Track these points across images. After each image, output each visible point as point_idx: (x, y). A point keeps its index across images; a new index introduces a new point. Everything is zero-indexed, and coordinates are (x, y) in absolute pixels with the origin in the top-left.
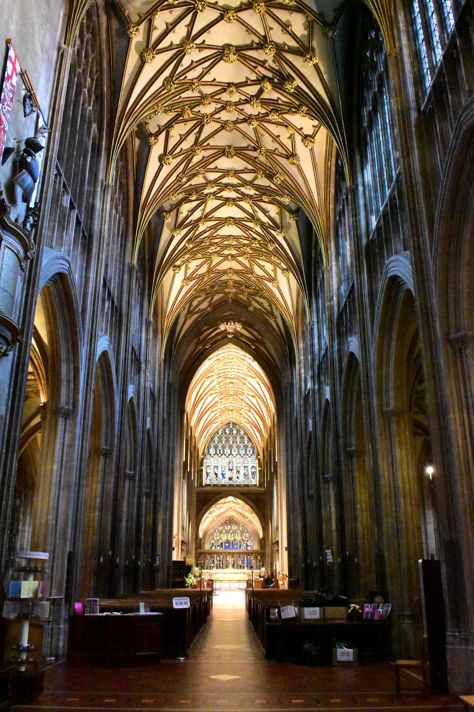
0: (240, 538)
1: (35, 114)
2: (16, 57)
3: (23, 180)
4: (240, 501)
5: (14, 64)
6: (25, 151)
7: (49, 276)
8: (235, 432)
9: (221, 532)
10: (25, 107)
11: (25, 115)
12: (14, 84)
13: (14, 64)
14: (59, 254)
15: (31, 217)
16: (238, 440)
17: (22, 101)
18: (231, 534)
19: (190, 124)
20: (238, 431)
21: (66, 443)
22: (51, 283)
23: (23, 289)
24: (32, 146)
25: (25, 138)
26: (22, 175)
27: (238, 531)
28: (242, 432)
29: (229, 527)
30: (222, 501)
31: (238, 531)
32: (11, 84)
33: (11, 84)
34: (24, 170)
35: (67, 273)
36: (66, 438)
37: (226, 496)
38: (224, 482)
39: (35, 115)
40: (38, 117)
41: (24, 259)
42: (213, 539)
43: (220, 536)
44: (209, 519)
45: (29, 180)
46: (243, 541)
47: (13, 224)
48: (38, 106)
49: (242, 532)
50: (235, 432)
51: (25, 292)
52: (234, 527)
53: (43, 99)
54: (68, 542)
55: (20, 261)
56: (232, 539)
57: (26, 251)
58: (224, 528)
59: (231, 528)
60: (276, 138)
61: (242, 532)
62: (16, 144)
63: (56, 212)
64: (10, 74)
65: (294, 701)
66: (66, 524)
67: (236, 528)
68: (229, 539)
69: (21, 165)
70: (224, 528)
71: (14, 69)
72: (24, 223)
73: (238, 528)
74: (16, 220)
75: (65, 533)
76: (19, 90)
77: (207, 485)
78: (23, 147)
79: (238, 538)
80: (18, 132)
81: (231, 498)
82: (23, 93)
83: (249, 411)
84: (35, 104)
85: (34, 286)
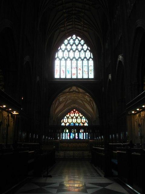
0: (80, 122)
9: (68, 118)
27: (79, 117)
29: (73, 115)
31: (79, 117)
42: (63, 122)
43: (68, 120)
46: (82, 123)
49: (81, 118)
52: (77, 115)
56: (75, 122)
58: (70, 115)
59: (75, 116)
61: (81, 118)
67: (77, 116)
68: (73, 122)
70: (70, 115)
73: (79, 115)
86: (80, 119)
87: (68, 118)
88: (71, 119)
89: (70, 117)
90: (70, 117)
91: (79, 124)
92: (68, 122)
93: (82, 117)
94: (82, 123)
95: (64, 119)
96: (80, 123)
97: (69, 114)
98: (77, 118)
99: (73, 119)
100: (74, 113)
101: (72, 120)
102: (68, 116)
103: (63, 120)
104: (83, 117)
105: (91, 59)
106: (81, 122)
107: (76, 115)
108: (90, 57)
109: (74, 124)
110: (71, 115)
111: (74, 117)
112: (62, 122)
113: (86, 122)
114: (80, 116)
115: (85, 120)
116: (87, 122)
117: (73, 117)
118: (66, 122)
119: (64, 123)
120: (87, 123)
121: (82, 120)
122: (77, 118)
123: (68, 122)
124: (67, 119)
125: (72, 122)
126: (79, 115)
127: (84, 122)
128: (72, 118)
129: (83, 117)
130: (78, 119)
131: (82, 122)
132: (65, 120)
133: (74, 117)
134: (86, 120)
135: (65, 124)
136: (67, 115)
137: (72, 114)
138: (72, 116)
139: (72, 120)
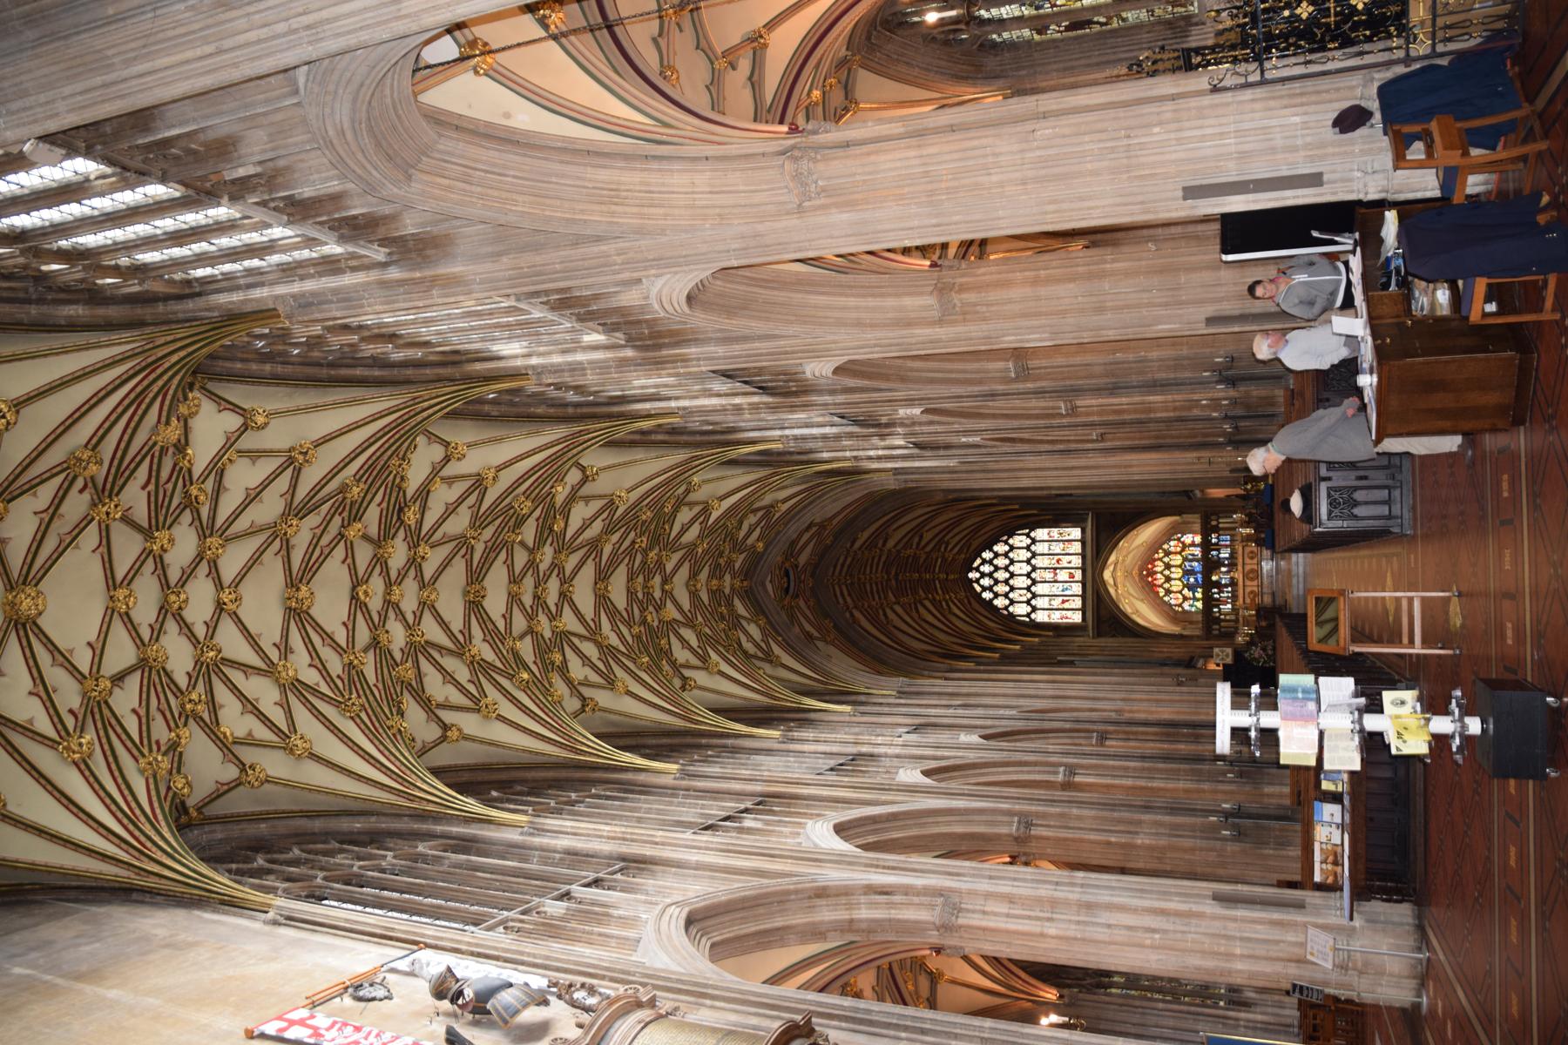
1: (388, 976)
2: (280, 1018)
3: (506, 1008)
4: (1112, 558)
5: (292, 1023)
6: (453, 1001)
7: (692, 949)
8: (986, 569)
9: (1168, 592)
10: (373, 999)
11: (389, 998)
12: (329, 1021)
13: (292, 1023)
14: (650, 928)
15: (576, 996)
16: (1001, 562)
17: (363, 1004)
19: (425, 666)
20: (984, 562)
21: (1005, 911)
22: (704, 940)
23: (712, 1007)
24: (445, 988)
25: (431, 1000)
26: (496, 1010)
28: (987, 555)
30: (1112, 591)
32: (328, 1029)
33: (328, 1029)
34: (488, 1006)
35: (686, 910)
36: (996, 910)
37: (1104, 582)
38: (1077, 589)
39: (391, 977)
40: (393, 971)
41: (654, 1006)
44: (1144, 614)
45: (506, 997)
47: (587, 1033)
48: (375, 971)
49: (1167, 553)
50: (986, 569)
51: (717, 1004)
52: (1159, 567)
53: (361, 958)
54: (1195, 908)
55: (661, 1017)
57: (639, 1005)
60: (451, 510)
61: (1167, 553)
62: (441, 1018)
63: (574, 930)
64: (310, 1031)
65: (1506, 494)
66: (1163, 912)
69: (480, 1008)
71: (302, 1022)
72: (587, 1009)
74: (580, 1026)
75: (1178, 914)
76: (343, 1010)
77: (1084, 618)
78: (445, 1004)
79: (1177, 560)
80: (419, 1014)
81: (1107, 575)
82: (347, 1001)
83: (947, 544)
84: (369, 979)
85: (706, 986)
87: (1168, 592)
91: (1185, 559)
98: (1168, 566)
102: (1162, 592)
105: (1033, 534)
107: (1159, 569)
108: (1028, 535)
109: (1187, 573)
122: (1168, 566)
128: (1168, 579)
132: (1174, 600)
135: (1185, 599)
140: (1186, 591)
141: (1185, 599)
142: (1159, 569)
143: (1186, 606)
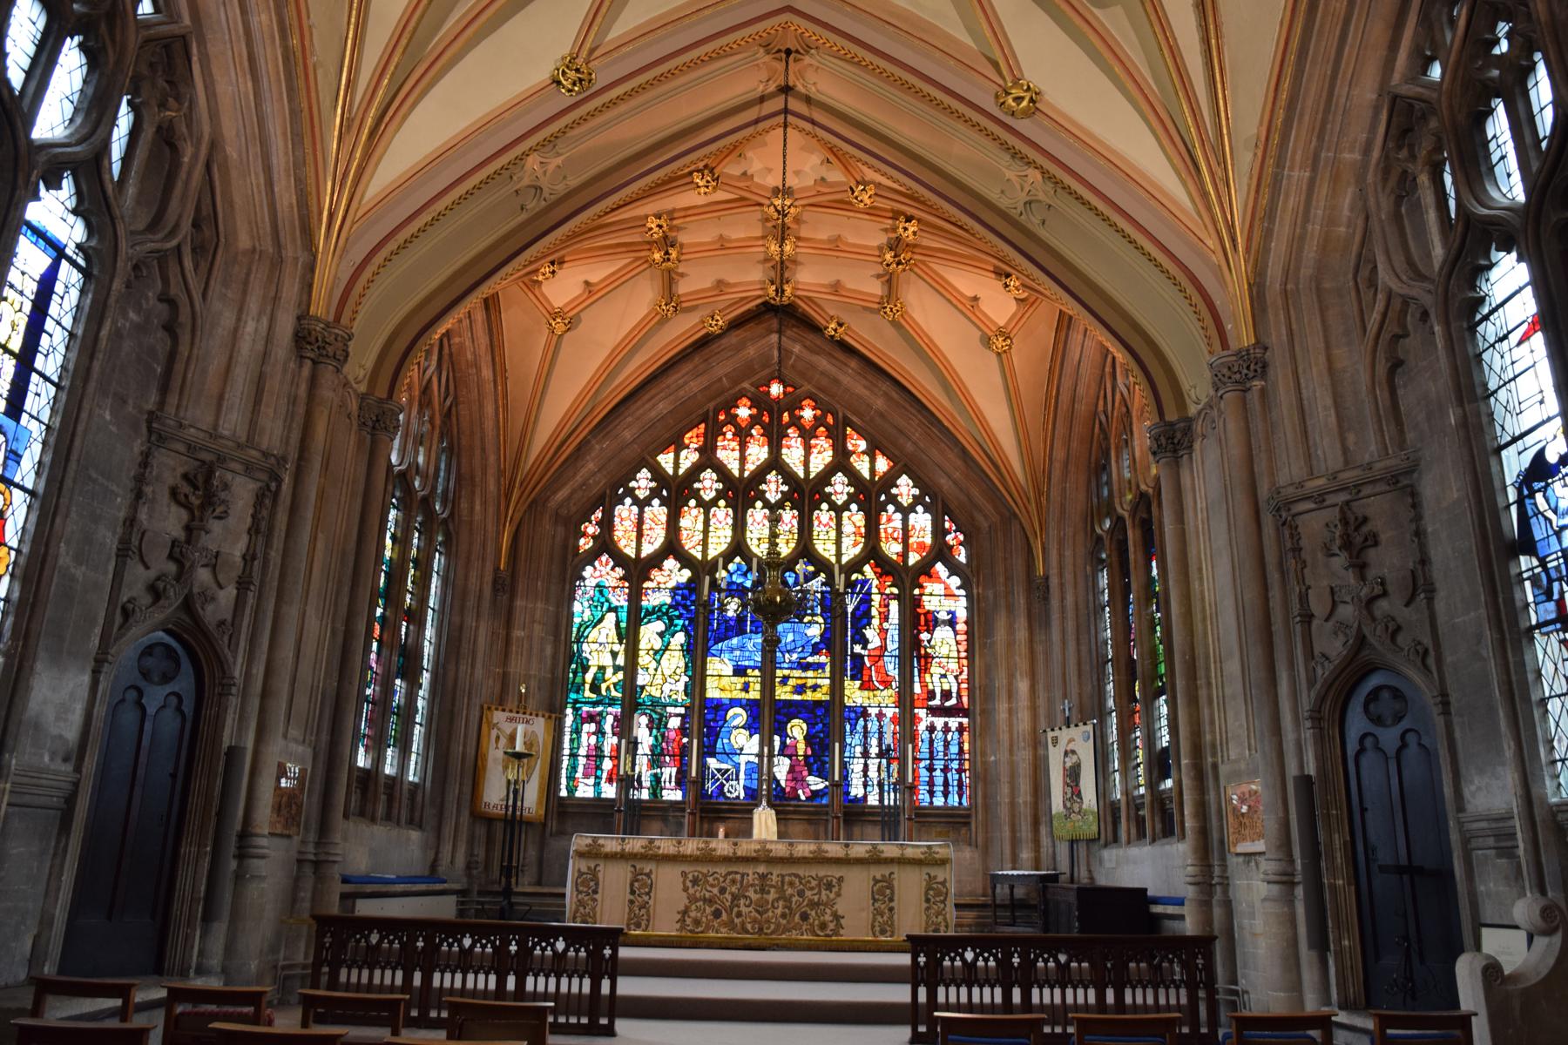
9: (676, 493)
18: (774, 508)
27: (840, 488)
29: (758, 453)
31: (840, 488)
42: (605, 544)
46: (886, 568)
49: (871, 497)
52: (806, 456)
58: (708, 459)
59: (775, 463)
61: (871, 497)
67: (822, 457)
68: (760, 549)
70: (708, 459)
73: (841, 462)
86: (855, 519)
87: (676, 493)
88: (722, 516)
89: (709, 484)
90: (709, 484)
92: (672, 547)
93: (890, 480)
94: (886, 568)
95: (625, 513)
96: (856, 565)
97: (693, 439)
98: (806, 495)
99: (757, 517)
100: (775, 441)
101: (739, 526)
103: (607, 524)
104: (904, 481)
106: (872, 552)
110: (728, 455)
111: (773, 488)
112: (585, 544)
113: (940, 552)
114: (862, 466)
115: (921, 521)
116: (962, 557)
117: (760, 475)
118: (655, 539)
119: (619, 559)
120: (954, 569)
121: (891, 522)
122: (806, 495)
123: (672, 547)
124: (657, 512)
125: (738, 547)
126: (841, 462)
127: (913, 558)
128: (741, 493)
129: (904, 481)
130: (824, 515)
131: (892, 549)
133: (773, 488)
134: (939, 532)
135: (637, 571)
136: (666, 460)
137: (743, 436)
138: (734, 468)
139: (739, 526)
140: (673, 574)
141: (637, 571)
142: (793, 454)
143: (601, 574)
